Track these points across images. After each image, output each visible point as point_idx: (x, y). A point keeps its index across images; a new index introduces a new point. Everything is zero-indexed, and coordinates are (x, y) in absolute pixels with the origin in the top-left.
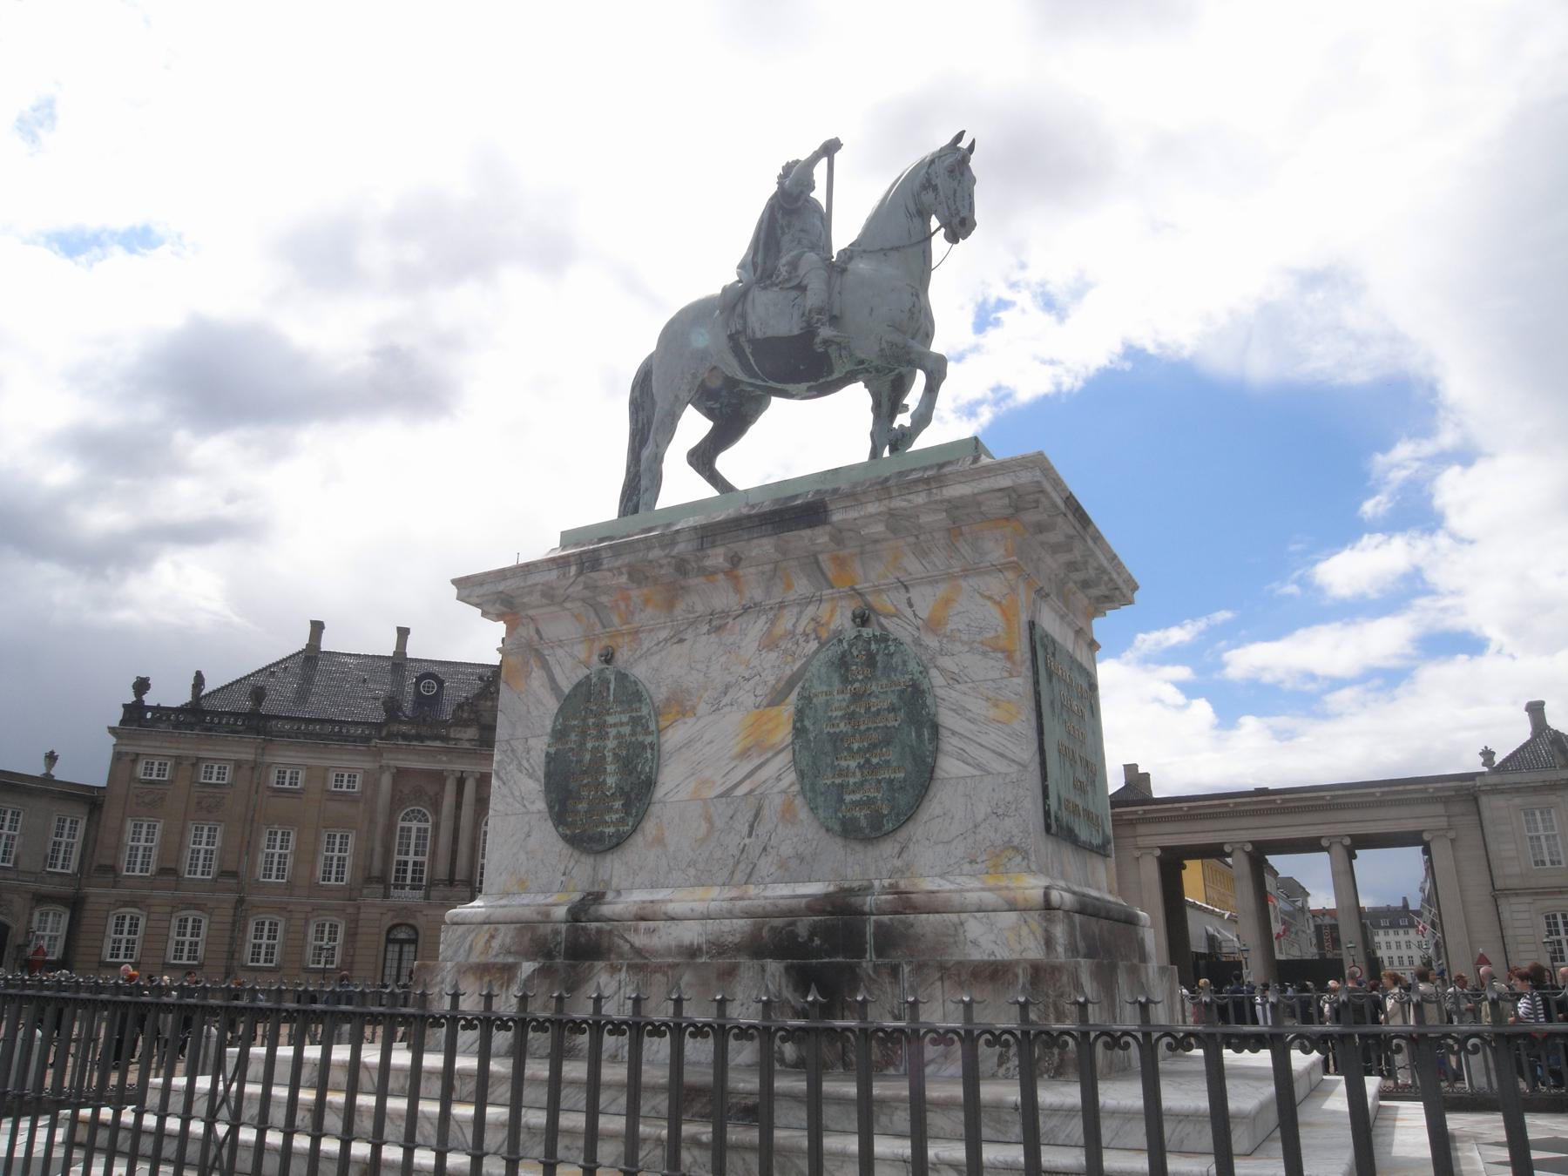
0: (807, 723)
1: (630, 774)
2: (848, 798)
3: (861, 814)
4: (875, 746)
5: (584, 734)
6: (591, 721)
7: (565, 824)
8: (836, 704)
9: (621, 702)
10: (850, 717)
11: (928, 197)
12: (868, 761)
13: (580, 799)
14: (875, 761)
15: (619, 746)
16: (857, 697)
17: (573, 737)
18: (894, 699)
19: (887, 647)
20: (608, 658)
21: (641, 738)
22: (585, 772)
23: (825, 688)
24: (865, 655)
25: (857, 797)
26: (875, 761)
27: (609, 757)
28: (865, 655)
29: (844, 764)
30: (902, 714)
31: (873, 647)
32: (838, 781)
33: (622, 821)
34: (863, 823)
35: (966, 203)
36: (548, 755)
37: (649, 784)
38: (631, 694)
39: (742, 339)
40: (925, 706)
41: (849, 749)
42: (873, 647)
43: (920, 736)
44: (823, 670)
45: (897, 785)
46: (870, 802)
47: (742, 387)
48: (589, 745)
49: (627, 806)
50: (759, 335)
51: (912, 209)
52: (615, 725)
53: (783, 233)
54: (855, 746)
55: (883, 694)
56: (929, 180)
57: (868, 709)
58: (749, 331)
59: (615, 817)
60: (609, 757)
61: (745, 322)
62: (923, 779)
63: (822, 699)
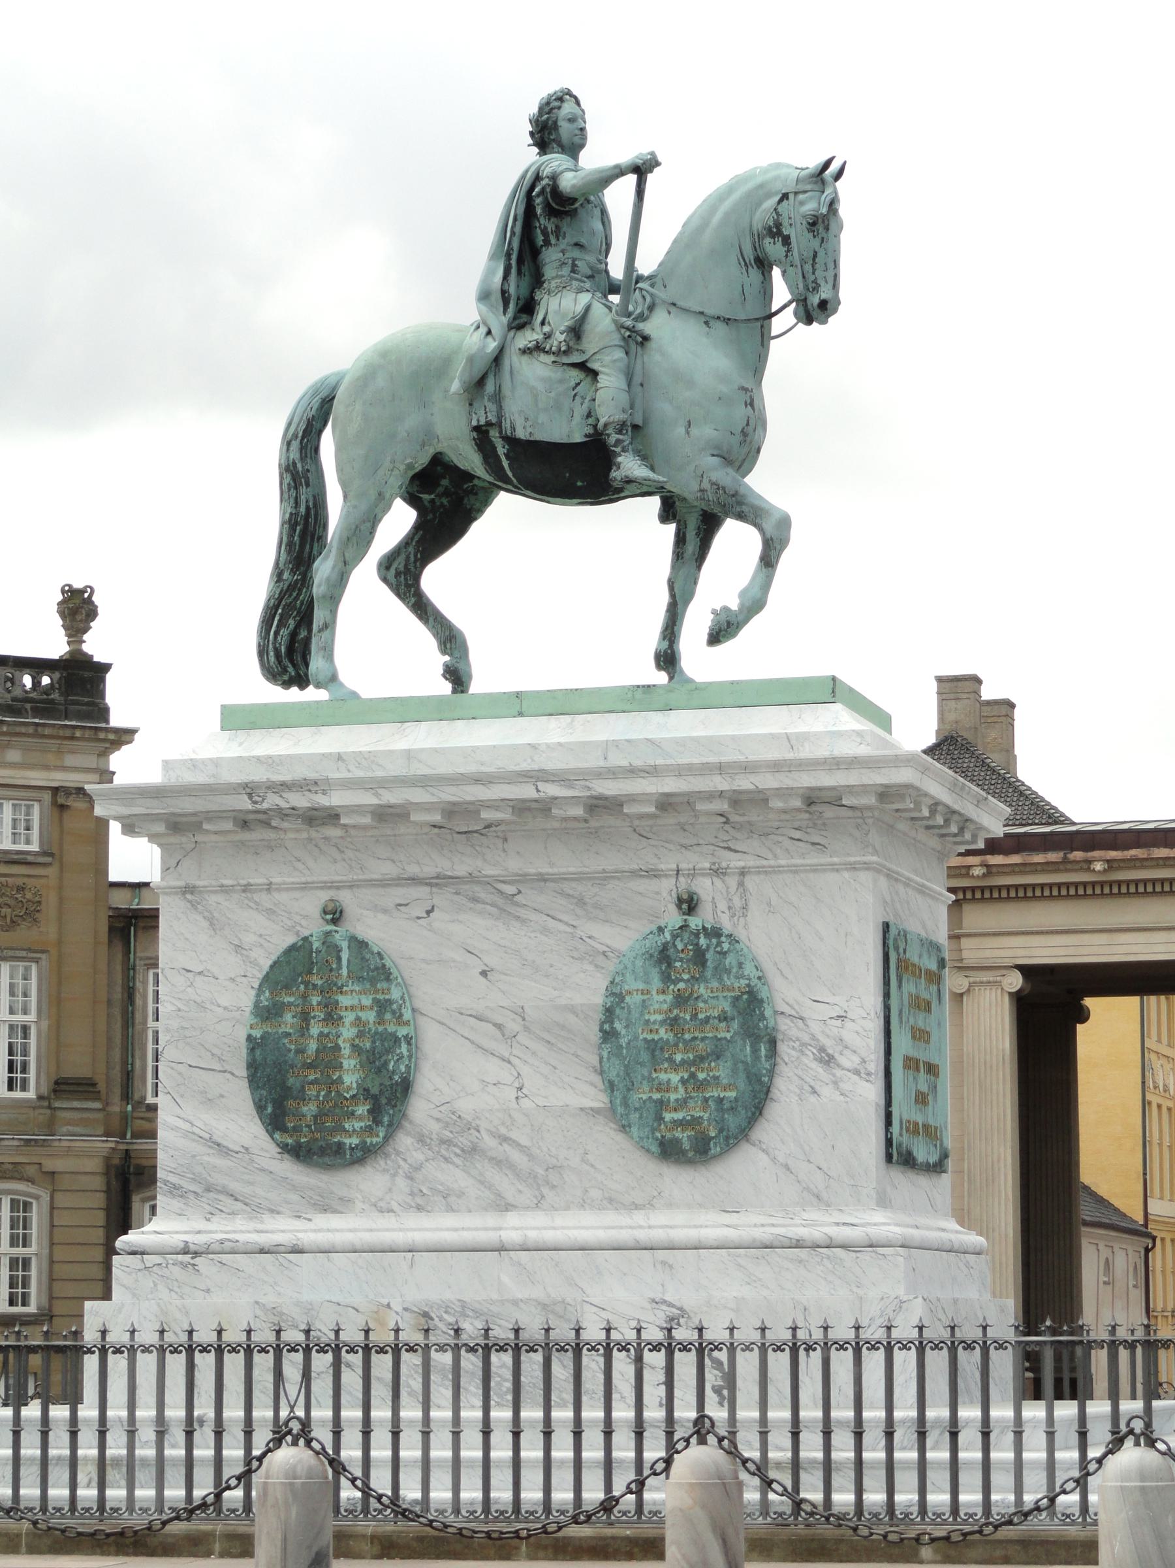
0: (618, 1025)
1: (379, 1071)
2: (668, 1116)
3: (684, 1136)
4: (702, 1059)
5: (305, 1017)
6: (315, 1000)
7: (283, 1129)
8: (656, 1006)
9: (360, 979)
10: (673, 1023)
11: (774, 248)
12: (693, 1076)
13: (302, 1098)
14: (701, 1076)
15: (360, 1035)
16: (681, 1000)
17: (288, 1017)
18: (726, 1006)
19: (719, 944)
20: (335, 915)
21: (391, 1028)
22: (310, 1066)
23: (641, 986)
24: (691, 953)
25: (679, 1116)
26: (701, 1076)
27: (346, 1051)
28: (691, 953)
29: (663, 1077)
30: (735, 1025)
31: (703, 941)
32: (656, 1096)
33: (369, 1130)
34: (686, 1145)
35: (830, 273)
36: (249, 1038)
37: (405, 1087)
38: (375, 970)
39: (494, 433)
40: (762, 1017)
41: (671, 1060)
42: (703, 941)
43: (755, 1051)
44: (639, 963)
45: (727, 1105)
46: (695, 1122)
47: (476, 482)
48: (315, 1030)
49: (376, 1113)
50: (521, 434)
51: (749, 254)
52: (352, 1008)
53: (547, 243)
54: (678, 1057)
55: (713, 999)
56: (778, 225)
57: (694, 1016)
58: (506, 425)
59: (358, 1125)
60: (346, 1051)
61: (500, 408)
62: (757, 1100)
63: (638, 998)
